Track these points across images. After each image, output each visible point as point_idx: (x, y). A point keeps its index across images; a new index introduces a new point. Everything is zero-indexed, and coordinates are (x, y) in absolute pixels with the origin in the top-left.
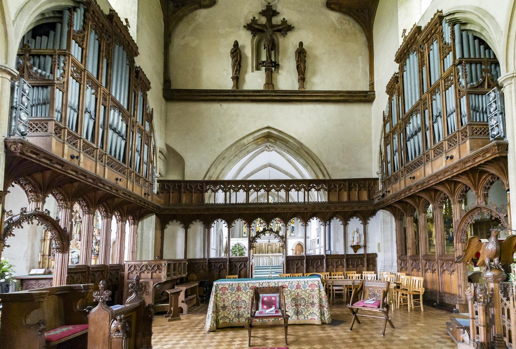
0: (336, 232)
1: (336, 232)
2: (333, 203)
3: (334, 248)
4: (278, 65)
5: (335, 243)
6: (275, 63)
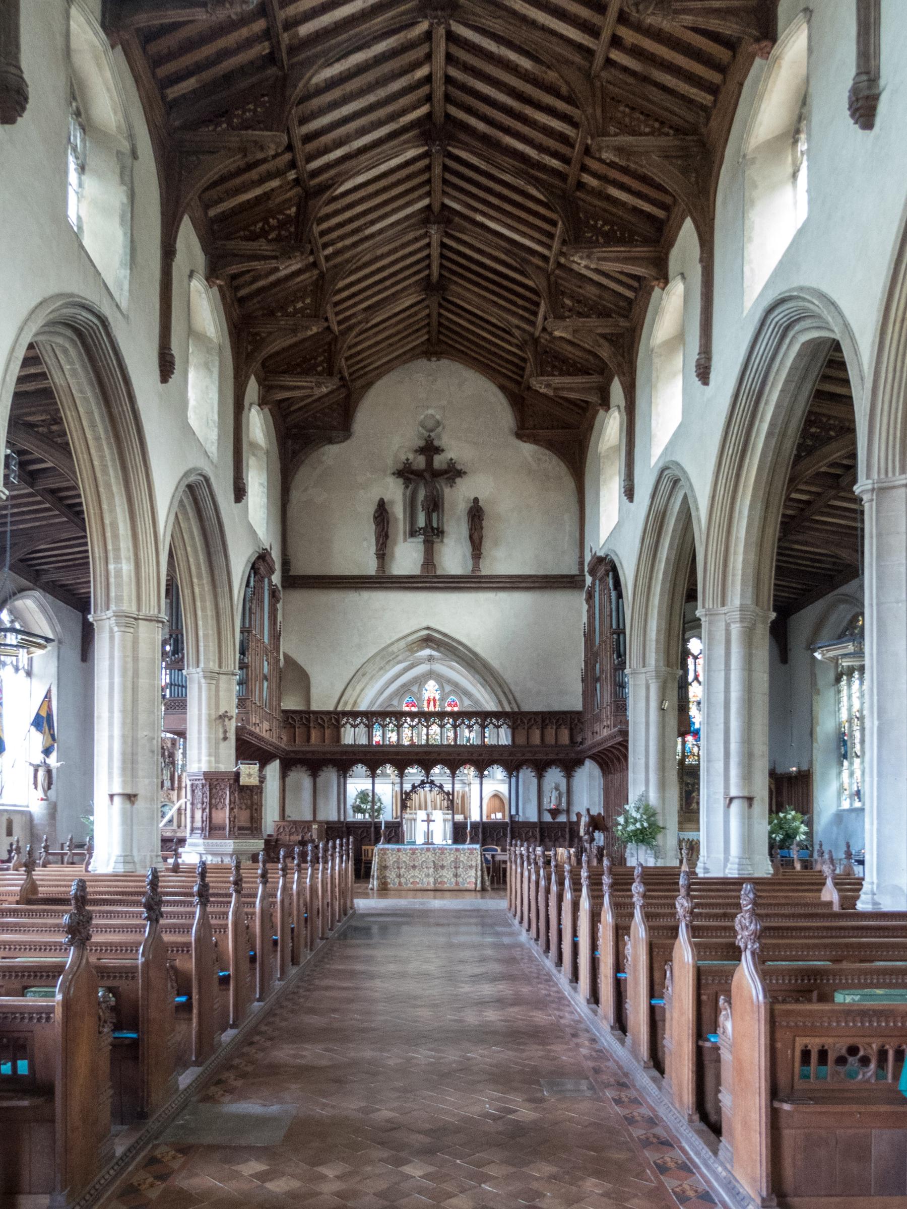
0: (527, 789)
1: (527, 789)
2: (519, 746)
3: (524, 813)
4: (442, 532)
5: (524, 804)
6: (437, 529)
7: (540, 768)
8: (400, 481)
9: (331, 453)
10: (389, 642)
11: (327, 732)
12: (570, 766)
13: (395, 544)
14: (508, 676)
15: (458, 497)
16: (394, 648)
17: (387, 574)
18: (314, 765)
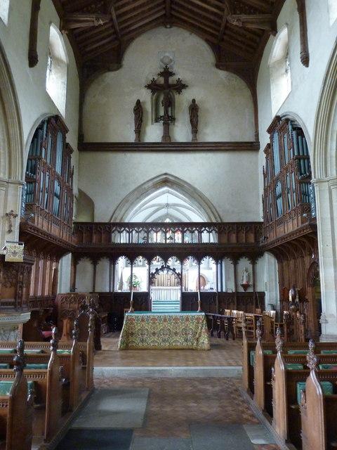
4: (174, 119)
7: (236, 260)
8: (149, 91)
9: (110, 76)
10: (142, 183)
11: (103, 236)
12: (255, 255)
13: (146, 125)
14: (215, 202)
15: (183, 100)
16: (146, 186)
17: (142, 141)
18: (95, 257)
